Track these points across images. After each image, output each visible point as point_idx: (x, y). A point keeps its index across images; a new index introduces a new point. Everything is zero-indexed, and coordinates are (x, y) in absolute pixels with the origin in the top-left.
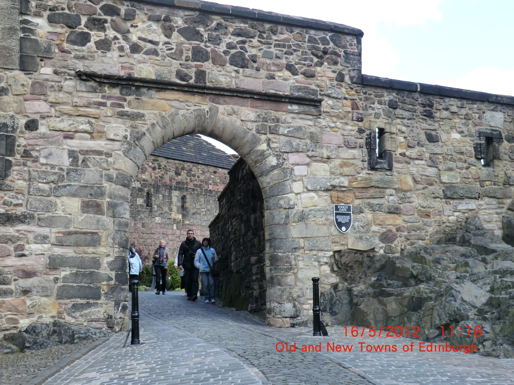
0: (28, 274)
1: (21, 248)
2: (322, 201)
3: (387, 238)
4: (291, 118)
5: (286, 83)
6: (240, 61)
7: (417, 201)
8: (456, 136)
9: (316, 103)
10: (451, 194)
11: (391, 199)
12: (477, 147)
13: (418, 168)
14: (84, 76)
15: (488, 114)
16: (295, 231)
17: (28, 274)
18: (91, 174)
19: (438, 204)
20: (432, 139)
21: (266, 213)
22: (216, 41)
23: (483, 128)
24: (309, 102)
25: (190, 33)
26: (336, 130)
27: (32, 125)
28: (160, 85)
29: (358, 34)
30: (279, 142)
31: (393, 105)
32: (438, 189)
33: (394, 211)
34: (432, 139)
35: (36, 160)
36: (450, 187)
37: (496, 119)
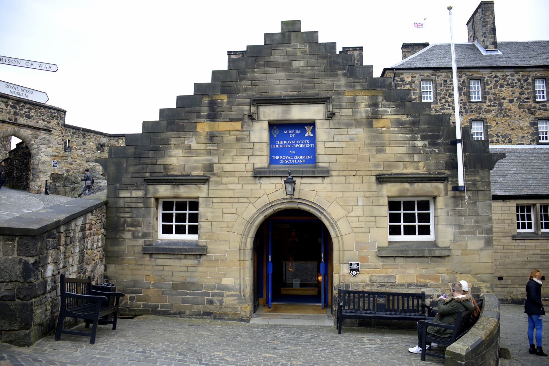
2: (49, 159)
3: (68, 171)
4: (42, 134)
6: (28, 116)
7: (78, 161)
8: (91, 144)
9: (50, 131)
10: (88, 160)
11: (70, 160)
13: (79, 152)
15: (102, 138)
19: (84, 163)
22: (21, 110)
23: (100, 142)
24: (48, 131)
25: (13, 107)
26: (56, 138)
29: (65, 112)
30: (38, 141)
32: (84, 159)
33: (71, 164)
34: (84, 144)
36: (88, 158)
37: (104, 140)
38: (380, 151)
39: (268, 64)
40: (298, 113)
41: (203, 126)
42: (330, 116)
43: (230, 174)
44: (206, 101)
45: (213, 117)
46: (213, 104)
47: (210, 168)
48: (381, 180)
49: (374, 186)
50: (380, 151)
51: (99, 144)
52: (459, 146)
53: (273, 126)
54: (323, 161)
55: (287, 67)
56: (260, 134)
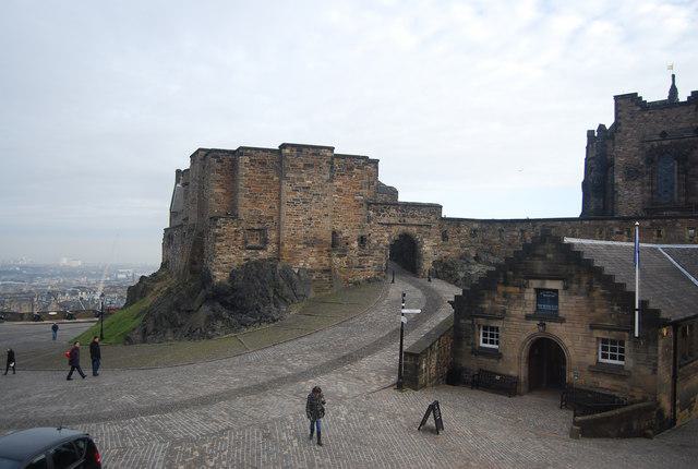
4: (424, 229)
6: (413, 216)
26: (435, 231)
38: (593, 311)
39: (535, 255)
40: (550, 285)
41: (501, 289)
42: (566, 288)
43: (515, 316)
44: (501, 274)
45: (506, 284)
46: (505, 277)
47: (504, 311)
48: (593, 327)
49: (589, 331)
50: (593, 311)
52: (637, 313)
53: (538, 291)
54: (562, 313)
55: (543, 257)
56: (530, 296)
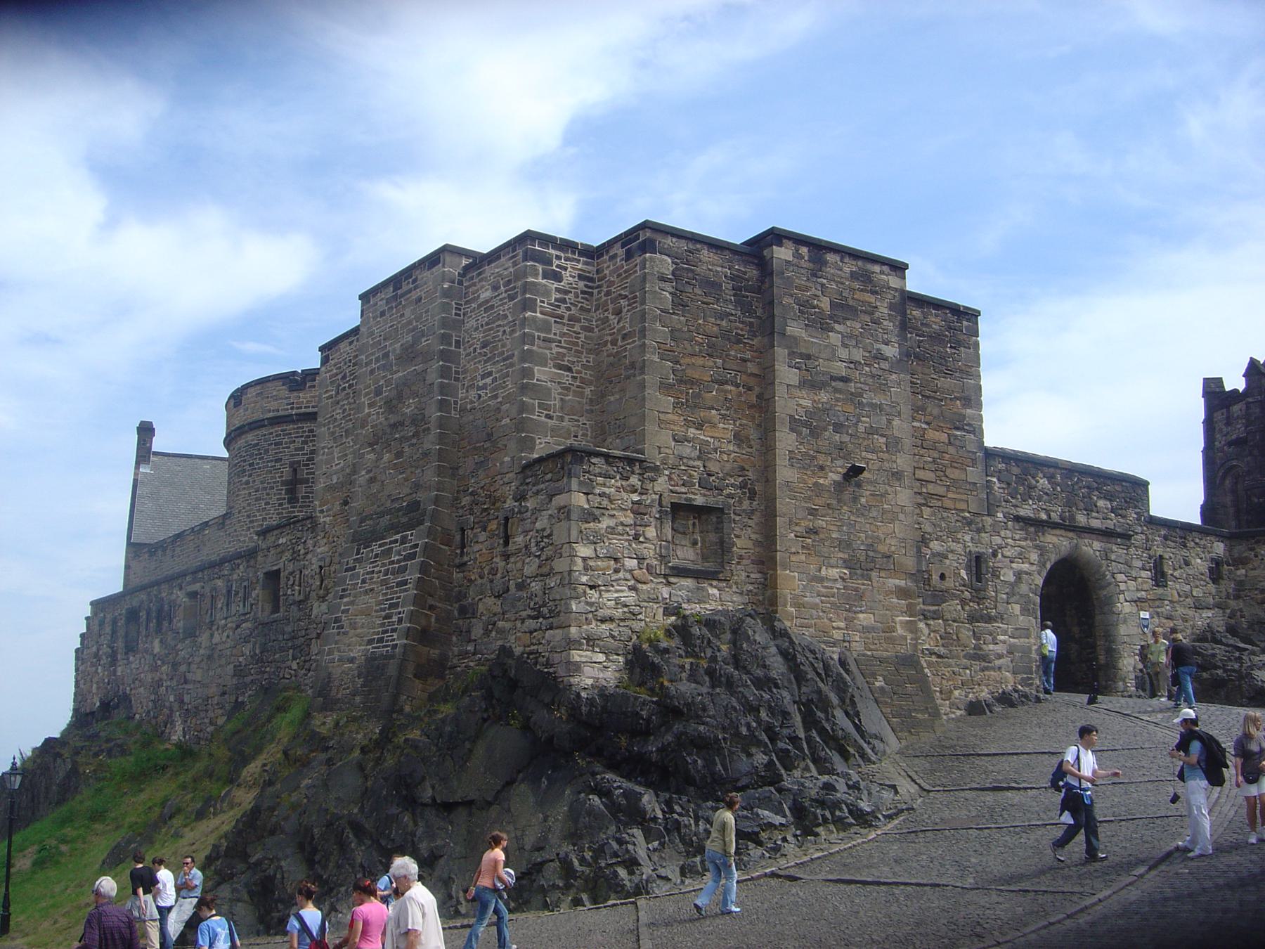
0: (1000, 656)
1: (994, 639)
5: (1113, 522)
7: (1180, 610)
12: (1211, 569)
14: (1017, 519)
16: (1123, 630)
17: (1000, 656)
18: (1024, 588)
19: (1191, 613)
20: (1187, 563)
21: (1098, 618)
27: (994, 554)
28: (1055, 526)
31: (1166, 538)
35: (998, 577)
36: (1197, 599)
51: (1212, 559)
